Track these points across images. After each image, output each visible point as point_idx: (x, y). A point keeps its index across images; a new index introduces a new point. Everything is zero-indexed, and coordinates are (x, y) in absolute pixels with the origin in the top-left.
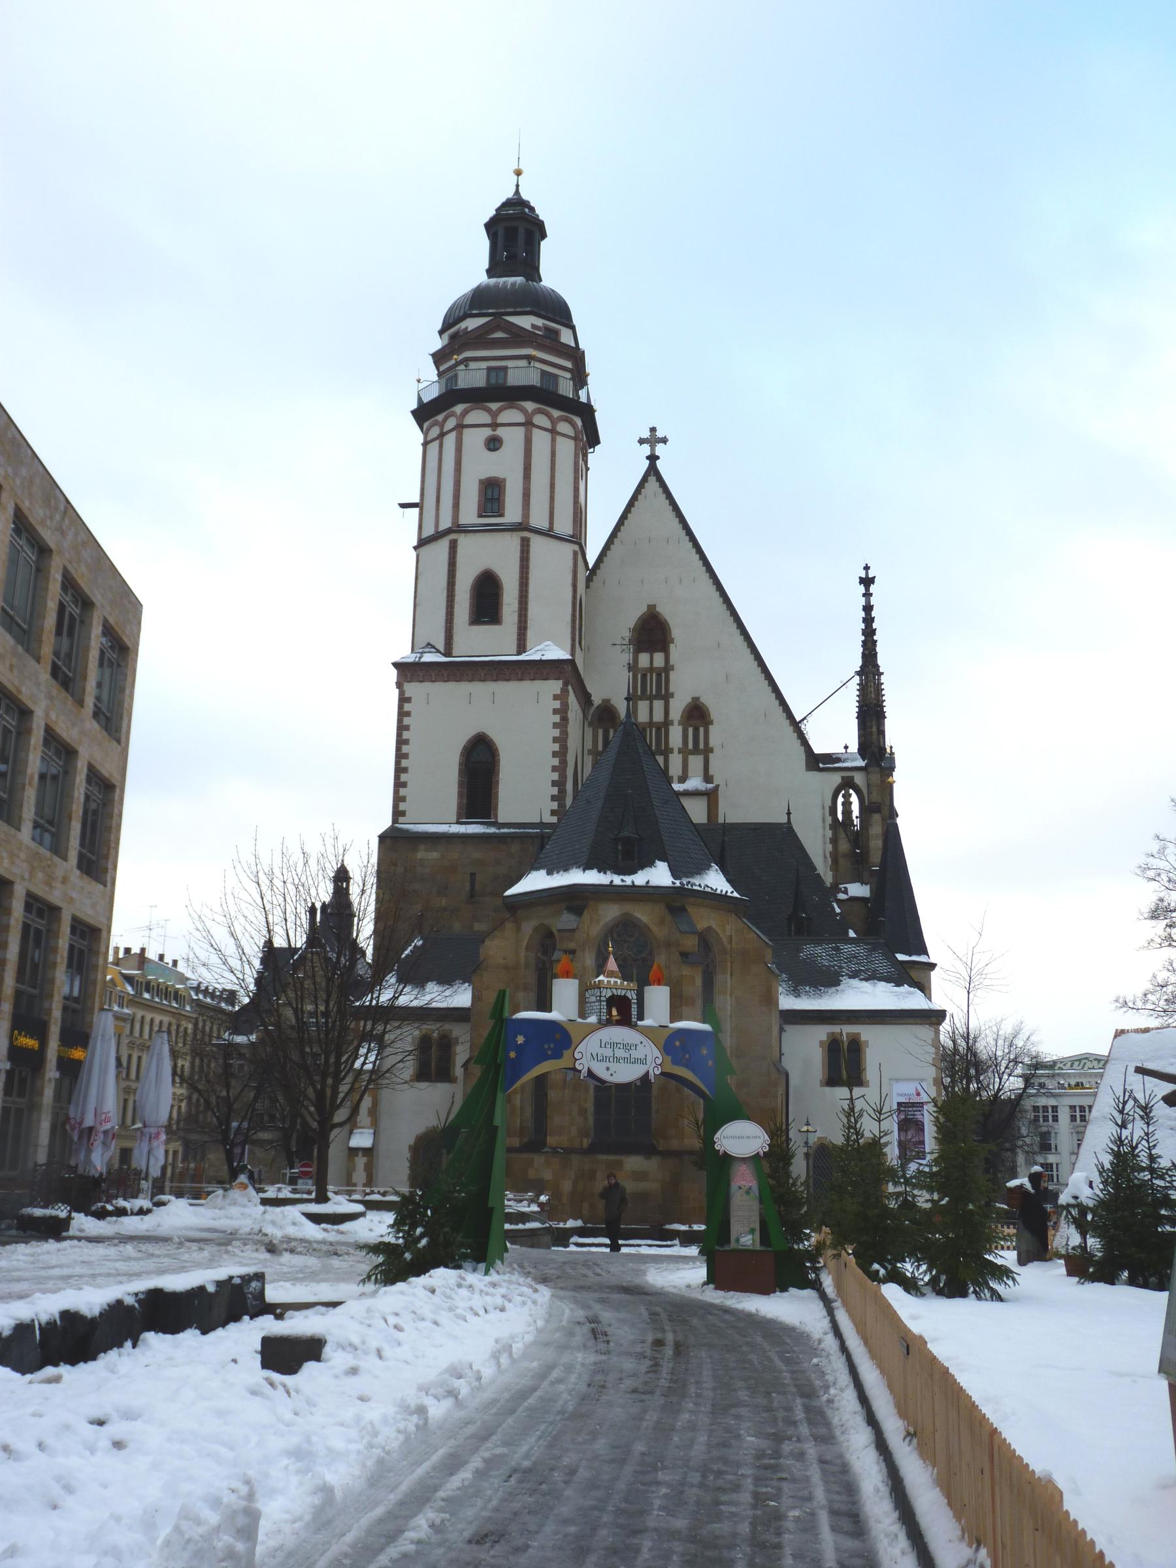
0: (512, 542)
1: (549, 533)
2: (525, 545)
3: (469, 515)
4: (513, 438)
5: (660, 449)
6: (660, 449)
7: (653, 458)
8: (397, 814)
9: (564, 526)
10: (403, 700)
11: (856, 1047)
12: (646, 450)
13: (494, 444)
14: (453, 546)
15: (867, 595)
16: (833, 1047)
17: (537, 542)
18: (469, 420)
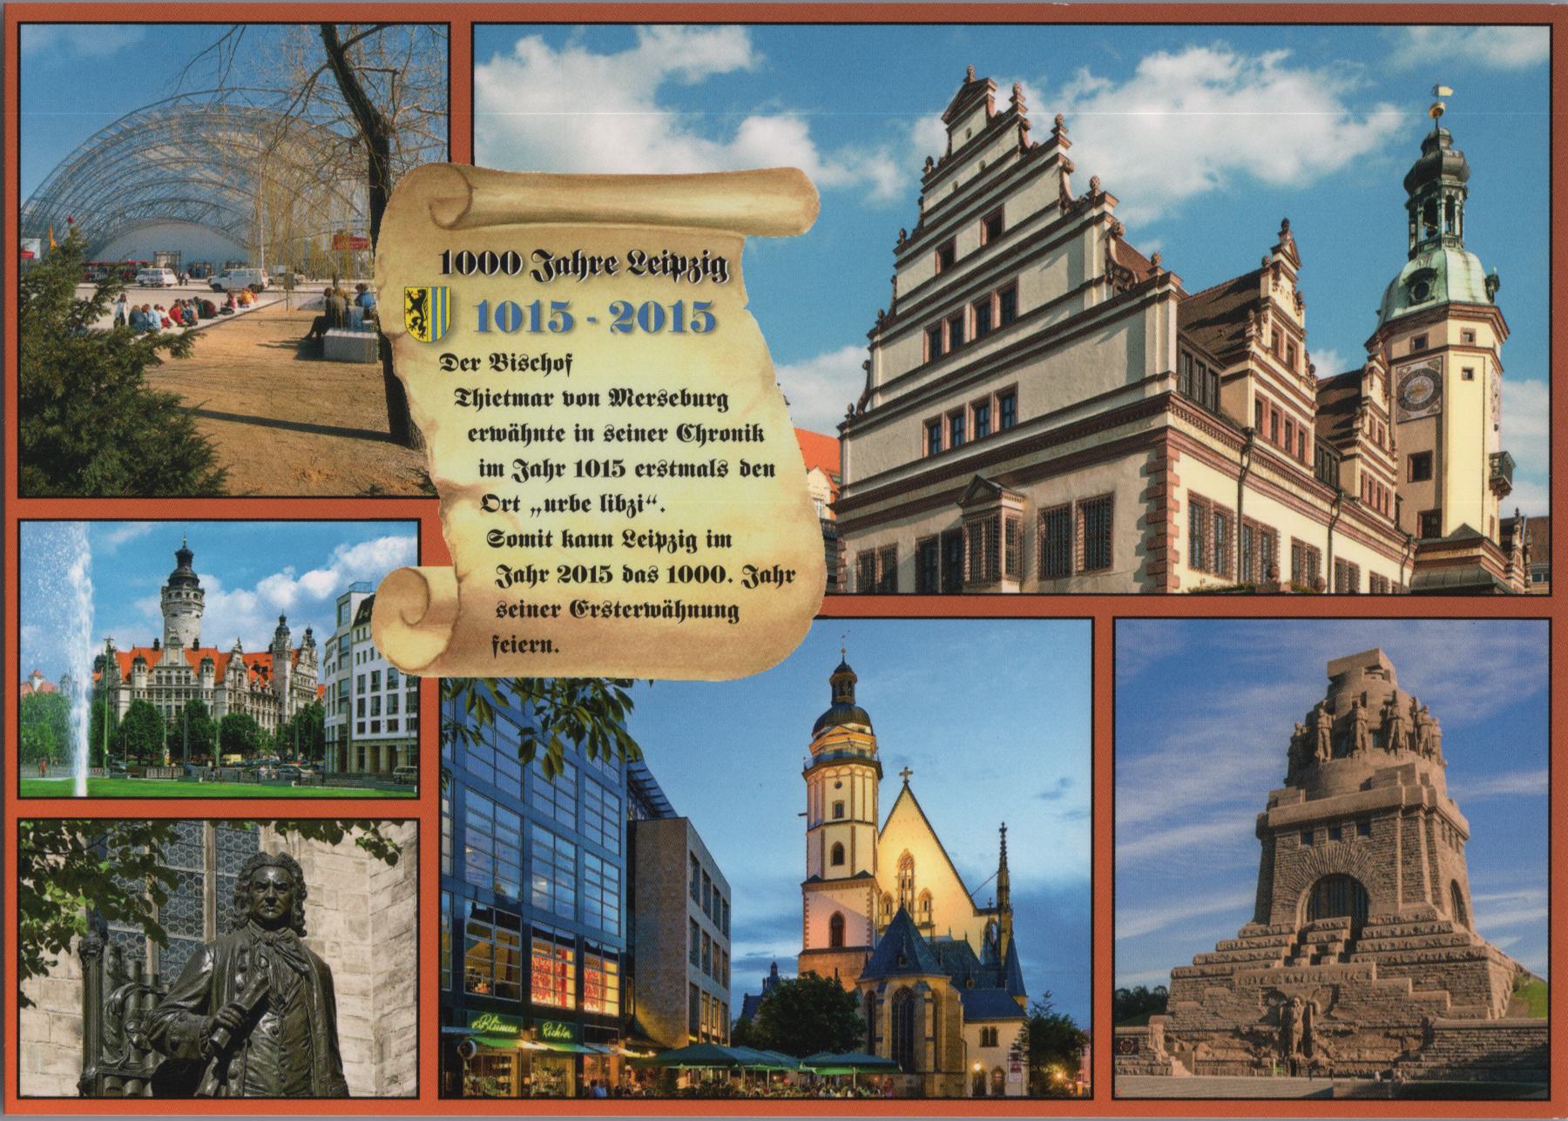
0: (846, 829)
1: (863, 822)
2: (853, 830)
3: (829, 817)
4: (846, 782)
5: (910, 777)
6: (910, 777)
7: (906, 782)
8: (805, 945)
9: (869, 818)
10: (805, 899)
11: (994, 1032)
12: (903, 778)
13: (838, 786)
14: (823, 834)
15: (1003, 836)
16: (985, 1032)
17: (860, 829)
18: (827, 774)
